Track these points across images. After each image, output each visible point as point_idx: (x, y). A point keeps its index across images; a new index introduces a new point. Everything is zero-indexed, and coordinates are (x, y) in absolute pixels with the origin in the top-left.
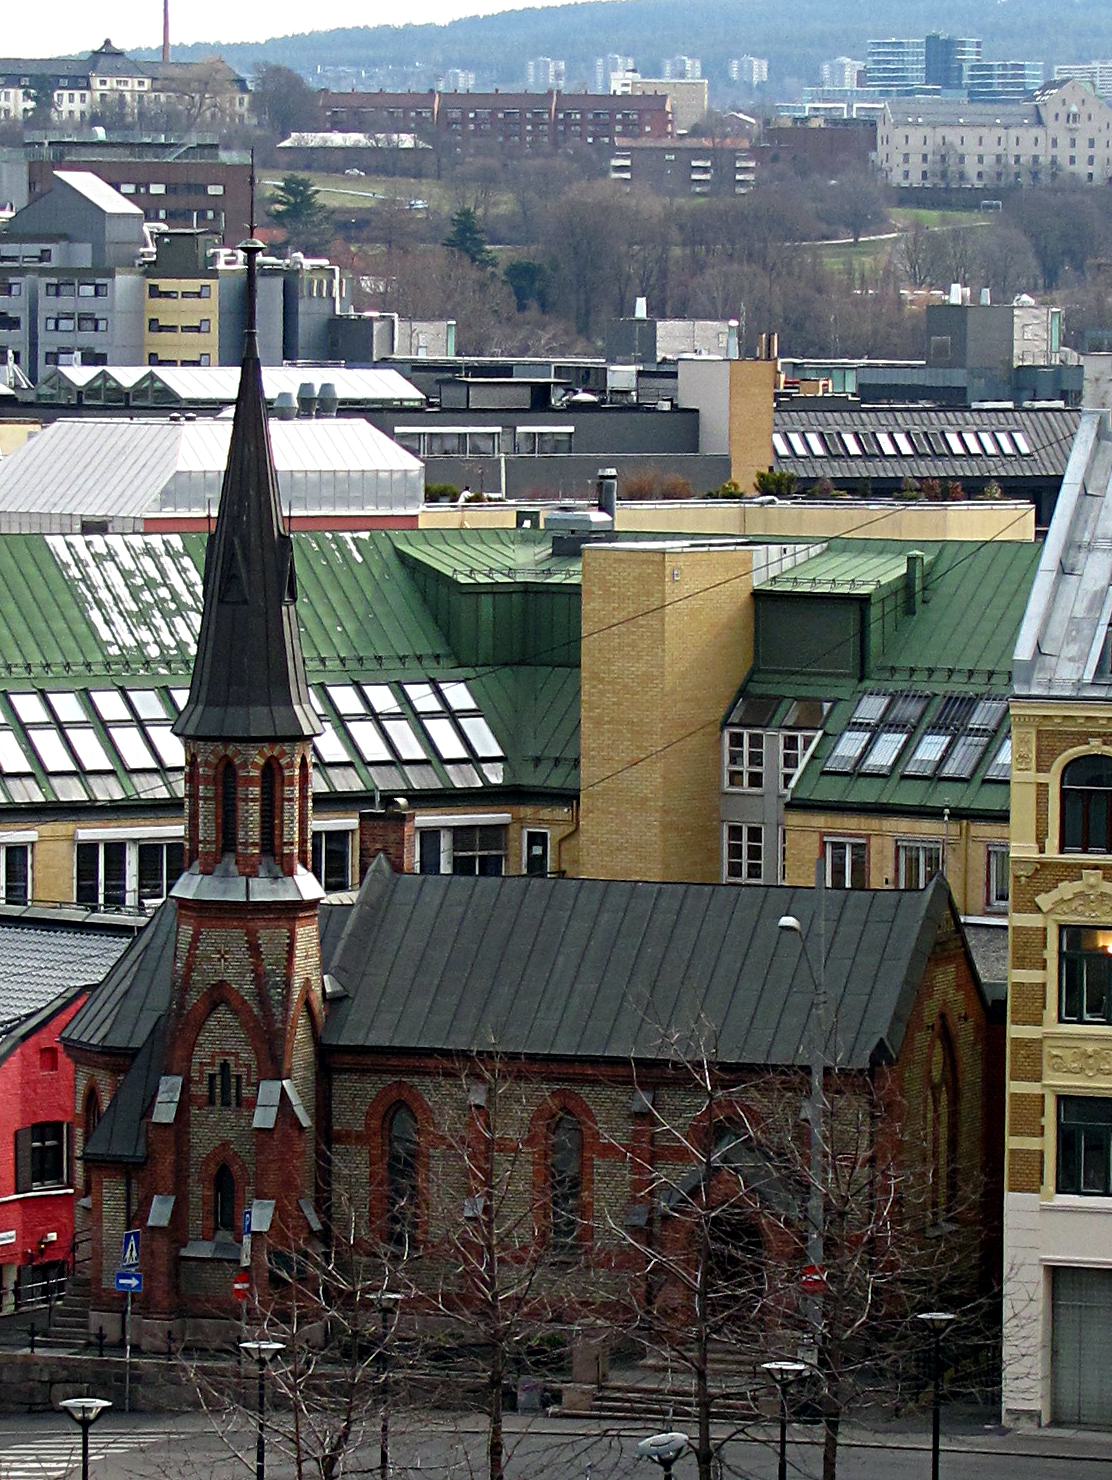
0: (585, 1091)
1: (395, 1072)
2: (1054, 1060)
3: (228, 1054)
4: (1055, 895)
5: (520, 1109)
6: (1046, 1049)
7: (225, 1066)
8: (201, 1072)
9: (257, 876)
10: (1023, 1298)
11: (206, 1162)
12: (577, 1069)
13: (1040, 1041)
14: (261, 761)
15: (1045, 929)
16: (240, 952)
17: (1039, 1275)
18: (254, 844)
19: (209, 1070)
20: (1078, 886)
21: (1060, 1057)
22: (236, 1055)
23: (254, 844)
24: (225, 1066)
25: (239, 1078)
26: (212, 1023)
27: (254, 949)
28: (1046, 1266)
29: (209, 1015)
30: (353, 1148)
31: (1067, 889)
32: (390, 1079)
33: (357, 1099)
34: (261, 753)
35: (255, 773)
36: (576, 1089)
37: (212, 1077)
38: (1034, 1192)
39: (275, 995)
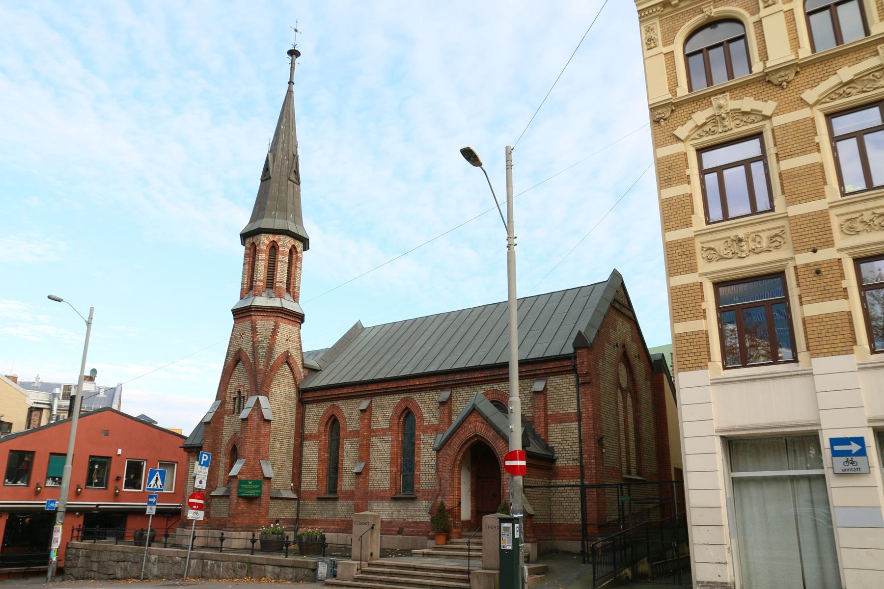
0: (417, 397)
1: (331, 400)
2: (708, 252)
4: (690, 125)
5: (385, 411)
6: (698, 246)
7: (239, 392)
10: (705, 479)
11: (228, 445)
12: (411, 382)
13: (691, 240)
15: (685, 154)
16: (248, 334)
17: (717, 446)
20: (709, 112)
21: (713, 249)
22: (243, 386)
24: (239, 392)
26: (236, 371)
27: (254, 330)
28: (721, 437)
30: (312, 443)
31: (700, 117)
32: (329, 404)
33: (315, 414)
34: (268, 239)
35: (264, 247)
36: (412, 395)
37: (235, 399)
38: (702, 368)
39: (261, 352)
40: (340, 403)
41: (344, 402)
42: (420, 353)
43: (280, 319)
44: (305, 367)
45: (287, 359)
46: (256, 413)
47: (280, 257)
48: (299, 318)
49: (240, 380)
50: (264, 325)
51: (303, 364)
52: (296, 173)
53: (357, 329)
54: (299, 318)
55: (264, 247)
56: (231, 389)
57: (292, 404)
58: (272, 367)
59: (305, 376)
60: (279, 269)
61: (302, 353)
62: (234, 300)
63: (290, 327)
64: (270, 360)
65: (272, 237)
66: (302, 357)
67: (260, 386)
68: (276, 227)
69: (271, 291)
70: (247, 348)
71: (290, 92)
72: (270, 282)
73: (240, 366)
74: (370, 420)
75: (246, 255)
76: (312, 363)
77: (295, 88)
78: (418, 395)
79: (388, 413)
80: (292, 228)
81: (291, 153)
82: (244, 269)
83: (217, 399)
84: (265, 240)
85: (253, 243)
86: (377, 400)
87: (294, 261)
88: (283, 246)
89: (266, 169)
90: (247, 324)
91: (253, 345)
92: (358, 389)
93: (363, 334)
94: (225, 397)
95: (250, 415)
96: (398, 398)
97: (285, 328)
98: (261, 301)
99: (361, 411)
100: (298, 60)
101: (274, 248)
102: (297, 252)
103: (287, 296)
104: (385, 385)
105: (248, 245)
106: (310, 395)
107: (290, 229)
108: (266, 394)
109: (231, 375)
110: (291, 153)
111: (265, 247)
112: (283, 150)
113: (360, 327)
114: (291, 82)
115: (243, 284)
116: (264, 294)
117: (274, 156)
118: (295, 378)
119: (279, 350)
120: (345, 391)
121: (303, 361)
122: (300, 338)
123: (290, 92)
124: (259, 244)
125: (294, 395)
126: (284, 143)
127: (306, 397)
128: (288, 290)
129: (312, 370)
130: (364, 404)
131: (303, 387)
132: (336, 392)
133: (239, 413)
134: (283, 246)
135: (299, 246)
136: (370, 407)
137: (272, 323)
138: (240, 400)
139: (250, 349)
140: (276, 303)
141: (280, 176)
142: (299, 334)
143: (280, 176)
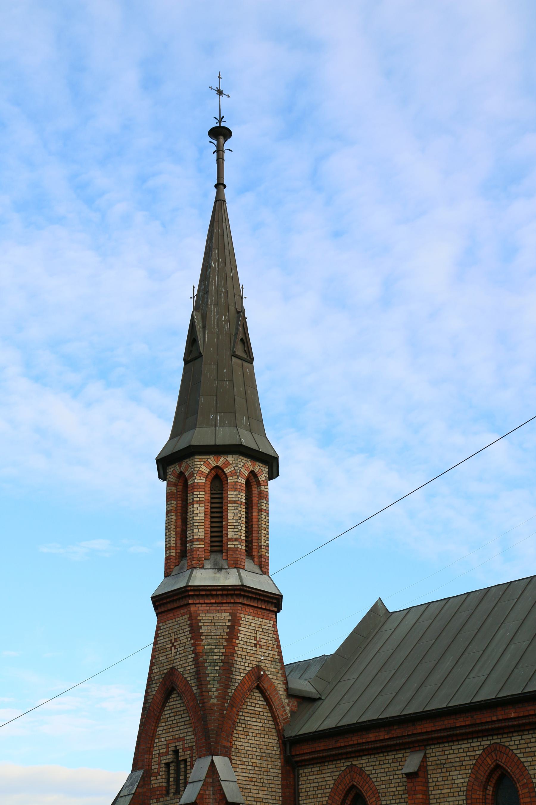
0: (515, 743)
1: (346, 756)
3: (179, 740)
8: (159, 764)
9: (202, 568)
14: (207, 471)
16: (186, 639)
18: (199, 540)
19: (165, 760)
22: (183, 739)
23: (199, 540)
25: (185, 760)
26: (167, 712)
27: (195, 631)
29: (164, 706)
32: (343, 765)
34: (206, 464)
35: (200, 480)
36: (505, 741)
37: (168, 765)
39: (212, 672)
40: (363, 762)
41: (372, 758)
42: (508, 656)
43: (240, 607)
44: (291, 694)
45: (258, 681)
46: (210, 791)
47: (231, 495)
48: (272, 603)
49: (176, 728)
50: (212, 620)
51: (287, 689)
52: (246, 342)
53: (378, 614)
54: (272, 603)
55: (200, 480)
56: (160, 746)
57: (274, 768)
58: (233, 698)
59: (292, 712)
60: (230, 515)
61: (283, 667)
62: (153, 577)
63: (259, 621)
64: (228, 687)
65: (213, 461)
66: (284, 675)
67: (214, 738)
68: (219, 442)
69: (218, 557)
70: (185, 666)
71: (220, 203)
72: (217, 541)
73: (174, 702)
74: (426, 793)
75: (170, 496)
76: (303, 685)
77: (228, 193)
78: (516, 739)
79: (460, 779)
80: (247, 440)
81: (232, 308)
82: (168, 522)
83: (135, 767)
84: (202, 466)
85: (182, 474)
86: (435, 753)
87: (255, 499)
88: (234, 473)
89: (192, 340)
90: (182, 621)
91: (196, 659)
92: (397, 732)
93: (391, 625)
94: (150, 764)
95: (200, 796)
96: (477, 747)
97: (250, 623)
98: (203, 577)
99: (409, 776)
100: (228, 145)
101: (218, 478)
102: (259, 483)
103: (248, 564)
104: (448, 723)
105: (172, 479)
106: (306, 748)
107: (244, 442)
108: (227, 753)
109: (158, 719)
110: (232, 308)
111: (202, 480)
112: (217, 304)
113: (382, 612)
114: (220, 185)
115: (168, 548)
116: (207, 565)
117: (204, 318)
118: (274, 718)
119: (243, 666)
120: (372, 736)
121: (286, 683)
122: (277, 640)
123: (220, 203)
124: (192, 475)
125: (276, 751)
126: (218, 291)
127: (297, 753)
128: (249, 553)
129: (304, 701)
130: (412, 762)
131: (291, 733)
132: (355, 740)
133: (178, 793)
134: (234, 473)
135: (262, 471)
136: (423, 767)
137: (227, 616)
138: (178, 767)
139: (190, 668)
140: (230, 579)
141: (217, 352)
142: (276, 632)
143: (217, 352)
